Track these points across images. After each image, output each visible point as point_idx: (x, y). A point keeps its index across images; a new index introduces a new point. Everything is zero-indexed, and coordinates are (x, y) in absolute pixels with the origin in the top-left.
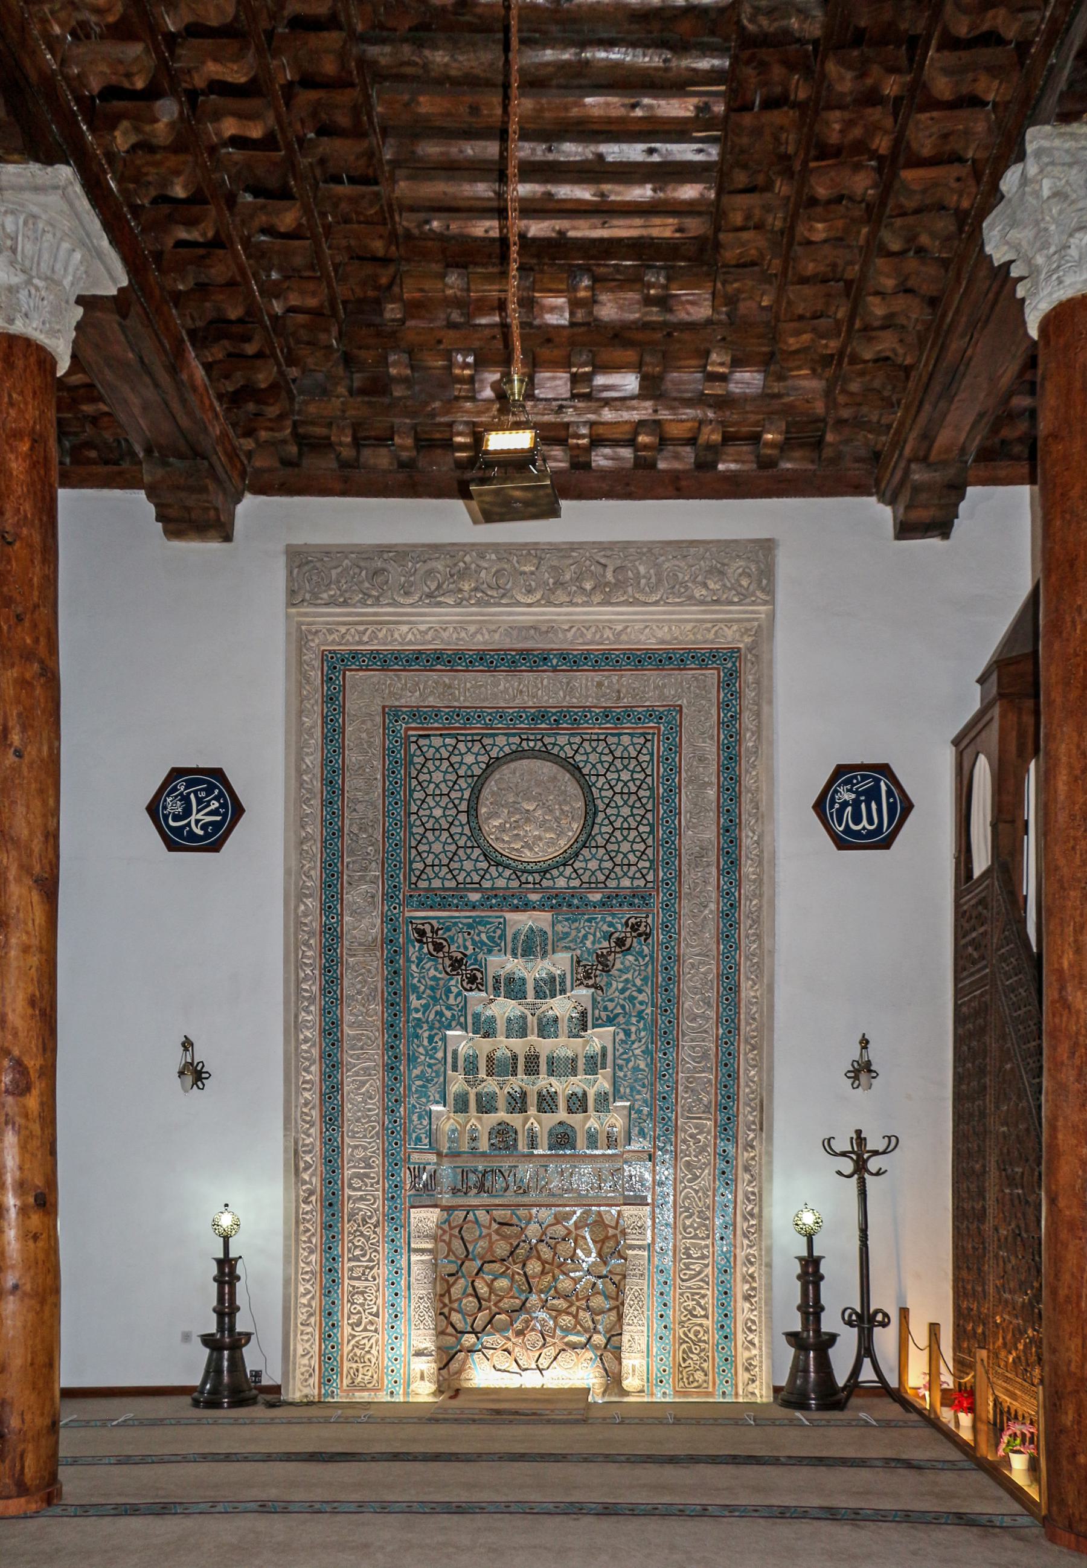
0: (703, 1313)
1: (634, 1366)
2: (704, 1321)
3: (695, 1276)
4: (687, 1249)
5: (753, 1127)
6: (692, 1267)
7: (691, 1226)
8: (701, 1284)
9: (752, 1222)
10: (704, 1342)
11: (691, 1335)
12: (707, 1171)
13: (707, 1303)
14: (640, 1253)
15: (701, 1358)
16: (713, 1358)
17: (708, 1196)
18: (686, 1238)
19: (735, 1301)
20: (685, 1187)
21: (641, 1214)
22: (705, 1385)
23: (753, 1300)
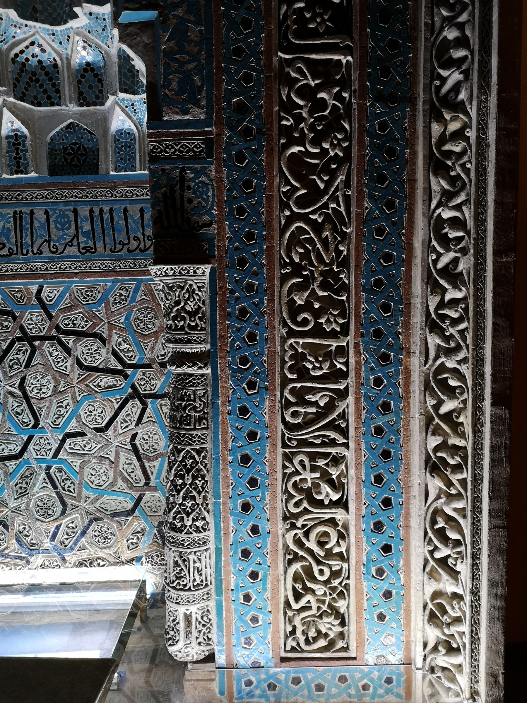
0: (335, 497)
1: (188, 618)
2: (340, 515)
3: (319, 417)
4: (298, 358)
6: (309, 397)
7: (308, 307)
8: (333, 435)
9: (452, 294)
10: (341, 556)
11: (312, 545)
12: (341, 178)
13: (344, 474)
14: (195, 370)
15: (334, 589)
16: (359, 591)
17: (344, 235)
18: (292, 334)
19: (408, 471)
20: (293, 218)
21: (193, 283)
22: (340, 644)
23: (455, 478)
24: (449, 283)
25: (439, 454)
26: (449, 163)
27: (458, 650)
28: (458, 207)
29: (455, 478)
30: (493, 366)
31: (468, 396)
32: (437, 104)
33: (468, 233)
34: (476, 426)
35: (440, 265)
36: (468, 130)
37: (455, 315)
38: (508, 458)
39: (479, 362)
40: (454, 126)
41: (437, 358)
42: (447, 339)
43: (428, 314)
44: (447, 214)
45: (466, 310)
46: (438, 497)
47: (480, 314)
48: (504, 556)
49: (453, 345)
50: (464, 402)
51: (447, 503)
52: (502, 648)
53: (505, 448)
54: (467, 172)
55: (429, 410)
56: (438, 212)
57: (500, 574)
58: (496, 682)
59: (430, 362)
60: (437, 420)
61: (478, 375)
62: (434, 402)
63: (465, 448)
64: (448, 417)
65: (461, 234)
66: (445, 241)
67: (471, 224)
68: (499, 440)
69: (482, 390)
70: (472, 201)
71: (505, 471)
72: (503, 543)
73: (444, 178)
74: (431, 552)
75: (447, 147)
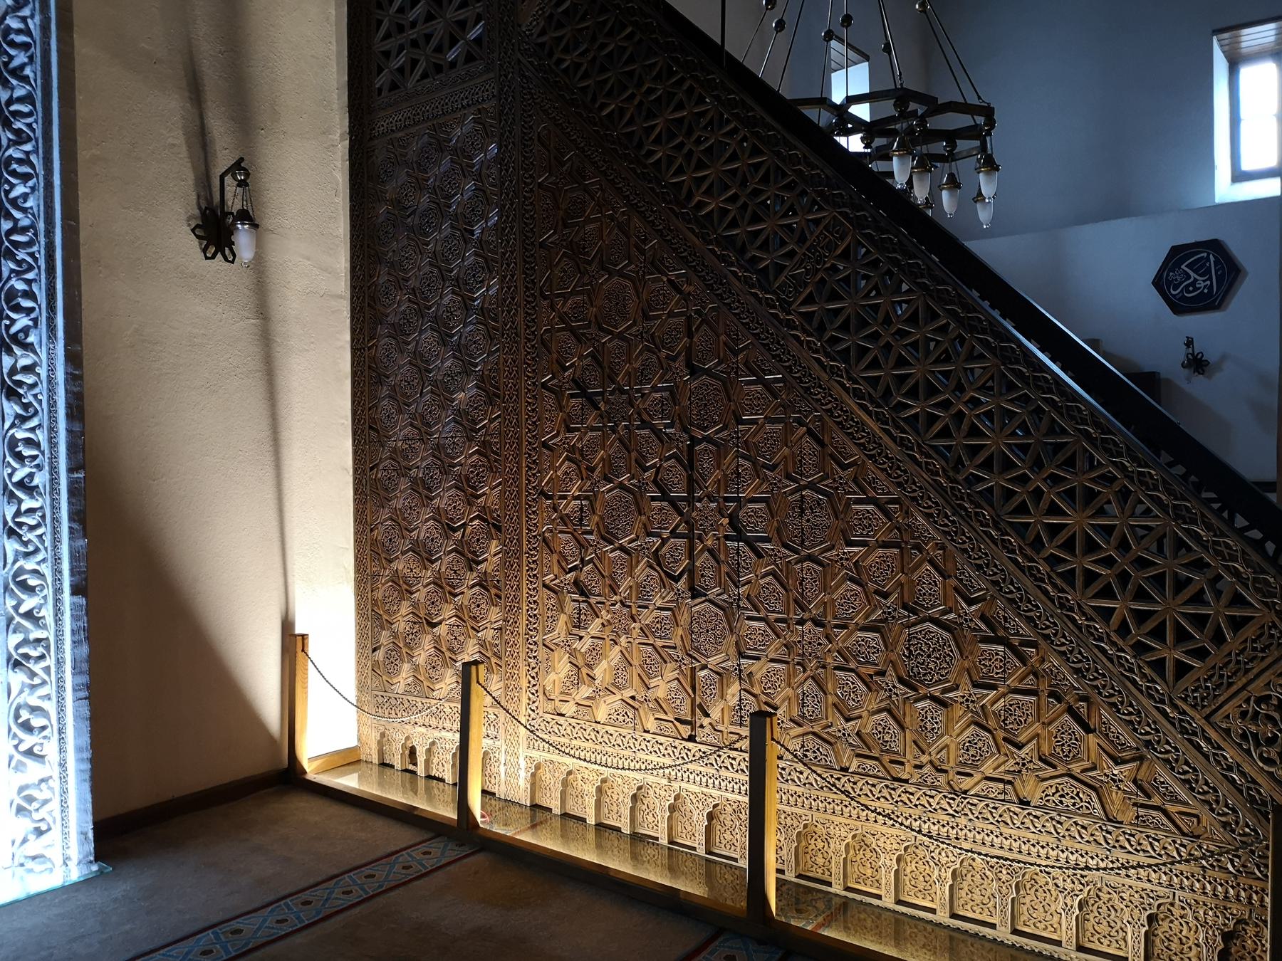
5: (27, 303)
9: (28, 503)
24: (26, 494)
25: (21, 651)
26: (21, 391)
27: (49, 829)
28: (32, 430)
29: (37, 668)
30: (71, 563)
31: (49, 592)
32: (7, 340)
33: (43, 453)
34: (57, 615)
35: (16, 478)
36: (38, 368)
37: (32, 522)
38: (87, 638)
39: (57, 560)
40: (23, 362)
41: (15, 562)
42: (25, 544)
43: (5, 523)
44: (20, 435)
45: (43, 517)
46: (21, 692)
47: (56, 520)
48: (88, 723)
49: (31, 548)
50: (45, 598)
51: (31, 694)
52: (90, 806)
53: (84, 630)
54: (40, 402)
55: (9, 612)
56: (11, 432)
57: (86, 740)
58: (85, 834)
59: (8, 566)
60: (18, 619)
61: (57, 572)
62: (14, 603)
63: (47, 639)
64: (29, 615)
65: (35, 452)
66: (19, 457)
67: (45, 445)
68: (78, 624)
69: (61, 584)
70: (45, 427)
71: (84, 650)
72: (86, 712)
73: (16, 403)
74: (16, 747)
75: (17, 377)
